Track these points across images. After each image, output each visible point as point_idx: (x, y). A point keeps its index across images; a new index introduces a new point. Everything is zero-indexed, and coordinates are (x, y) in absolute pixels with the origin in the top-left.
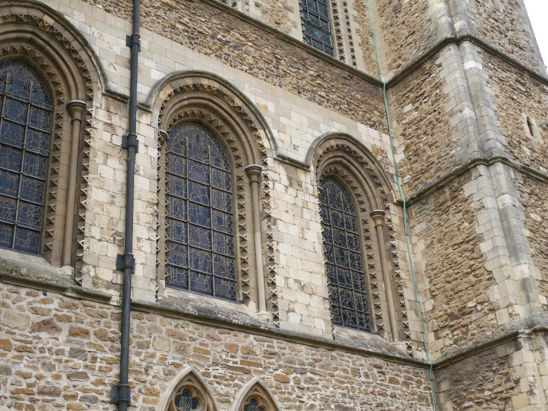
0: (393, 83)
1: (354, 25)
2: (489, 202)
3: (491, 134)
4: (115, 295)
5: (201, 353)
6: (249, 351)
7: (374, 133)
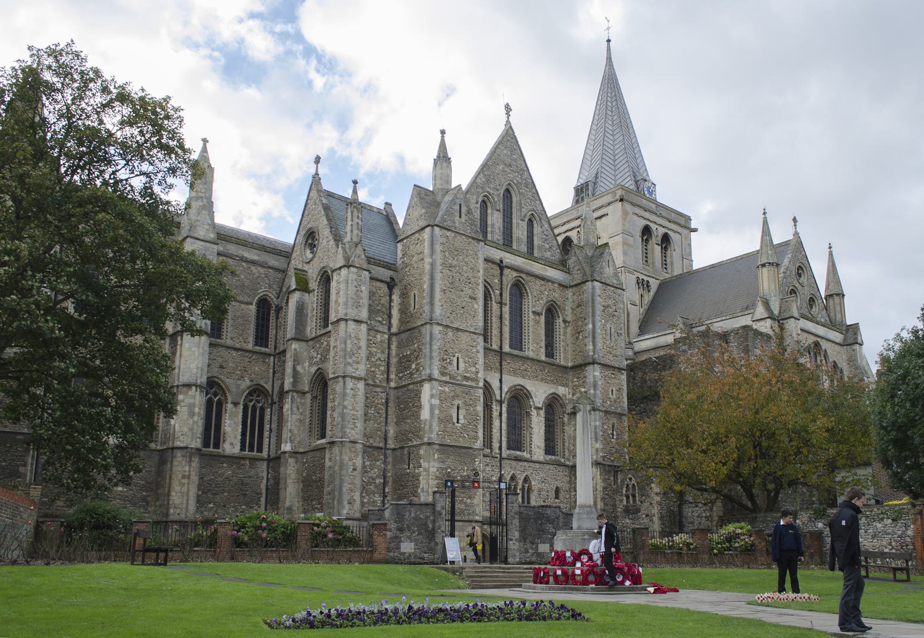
0: (573, 368)
1: (562, 343)
4: (498, 456)
6: (525, 466)
7: (563, 388)
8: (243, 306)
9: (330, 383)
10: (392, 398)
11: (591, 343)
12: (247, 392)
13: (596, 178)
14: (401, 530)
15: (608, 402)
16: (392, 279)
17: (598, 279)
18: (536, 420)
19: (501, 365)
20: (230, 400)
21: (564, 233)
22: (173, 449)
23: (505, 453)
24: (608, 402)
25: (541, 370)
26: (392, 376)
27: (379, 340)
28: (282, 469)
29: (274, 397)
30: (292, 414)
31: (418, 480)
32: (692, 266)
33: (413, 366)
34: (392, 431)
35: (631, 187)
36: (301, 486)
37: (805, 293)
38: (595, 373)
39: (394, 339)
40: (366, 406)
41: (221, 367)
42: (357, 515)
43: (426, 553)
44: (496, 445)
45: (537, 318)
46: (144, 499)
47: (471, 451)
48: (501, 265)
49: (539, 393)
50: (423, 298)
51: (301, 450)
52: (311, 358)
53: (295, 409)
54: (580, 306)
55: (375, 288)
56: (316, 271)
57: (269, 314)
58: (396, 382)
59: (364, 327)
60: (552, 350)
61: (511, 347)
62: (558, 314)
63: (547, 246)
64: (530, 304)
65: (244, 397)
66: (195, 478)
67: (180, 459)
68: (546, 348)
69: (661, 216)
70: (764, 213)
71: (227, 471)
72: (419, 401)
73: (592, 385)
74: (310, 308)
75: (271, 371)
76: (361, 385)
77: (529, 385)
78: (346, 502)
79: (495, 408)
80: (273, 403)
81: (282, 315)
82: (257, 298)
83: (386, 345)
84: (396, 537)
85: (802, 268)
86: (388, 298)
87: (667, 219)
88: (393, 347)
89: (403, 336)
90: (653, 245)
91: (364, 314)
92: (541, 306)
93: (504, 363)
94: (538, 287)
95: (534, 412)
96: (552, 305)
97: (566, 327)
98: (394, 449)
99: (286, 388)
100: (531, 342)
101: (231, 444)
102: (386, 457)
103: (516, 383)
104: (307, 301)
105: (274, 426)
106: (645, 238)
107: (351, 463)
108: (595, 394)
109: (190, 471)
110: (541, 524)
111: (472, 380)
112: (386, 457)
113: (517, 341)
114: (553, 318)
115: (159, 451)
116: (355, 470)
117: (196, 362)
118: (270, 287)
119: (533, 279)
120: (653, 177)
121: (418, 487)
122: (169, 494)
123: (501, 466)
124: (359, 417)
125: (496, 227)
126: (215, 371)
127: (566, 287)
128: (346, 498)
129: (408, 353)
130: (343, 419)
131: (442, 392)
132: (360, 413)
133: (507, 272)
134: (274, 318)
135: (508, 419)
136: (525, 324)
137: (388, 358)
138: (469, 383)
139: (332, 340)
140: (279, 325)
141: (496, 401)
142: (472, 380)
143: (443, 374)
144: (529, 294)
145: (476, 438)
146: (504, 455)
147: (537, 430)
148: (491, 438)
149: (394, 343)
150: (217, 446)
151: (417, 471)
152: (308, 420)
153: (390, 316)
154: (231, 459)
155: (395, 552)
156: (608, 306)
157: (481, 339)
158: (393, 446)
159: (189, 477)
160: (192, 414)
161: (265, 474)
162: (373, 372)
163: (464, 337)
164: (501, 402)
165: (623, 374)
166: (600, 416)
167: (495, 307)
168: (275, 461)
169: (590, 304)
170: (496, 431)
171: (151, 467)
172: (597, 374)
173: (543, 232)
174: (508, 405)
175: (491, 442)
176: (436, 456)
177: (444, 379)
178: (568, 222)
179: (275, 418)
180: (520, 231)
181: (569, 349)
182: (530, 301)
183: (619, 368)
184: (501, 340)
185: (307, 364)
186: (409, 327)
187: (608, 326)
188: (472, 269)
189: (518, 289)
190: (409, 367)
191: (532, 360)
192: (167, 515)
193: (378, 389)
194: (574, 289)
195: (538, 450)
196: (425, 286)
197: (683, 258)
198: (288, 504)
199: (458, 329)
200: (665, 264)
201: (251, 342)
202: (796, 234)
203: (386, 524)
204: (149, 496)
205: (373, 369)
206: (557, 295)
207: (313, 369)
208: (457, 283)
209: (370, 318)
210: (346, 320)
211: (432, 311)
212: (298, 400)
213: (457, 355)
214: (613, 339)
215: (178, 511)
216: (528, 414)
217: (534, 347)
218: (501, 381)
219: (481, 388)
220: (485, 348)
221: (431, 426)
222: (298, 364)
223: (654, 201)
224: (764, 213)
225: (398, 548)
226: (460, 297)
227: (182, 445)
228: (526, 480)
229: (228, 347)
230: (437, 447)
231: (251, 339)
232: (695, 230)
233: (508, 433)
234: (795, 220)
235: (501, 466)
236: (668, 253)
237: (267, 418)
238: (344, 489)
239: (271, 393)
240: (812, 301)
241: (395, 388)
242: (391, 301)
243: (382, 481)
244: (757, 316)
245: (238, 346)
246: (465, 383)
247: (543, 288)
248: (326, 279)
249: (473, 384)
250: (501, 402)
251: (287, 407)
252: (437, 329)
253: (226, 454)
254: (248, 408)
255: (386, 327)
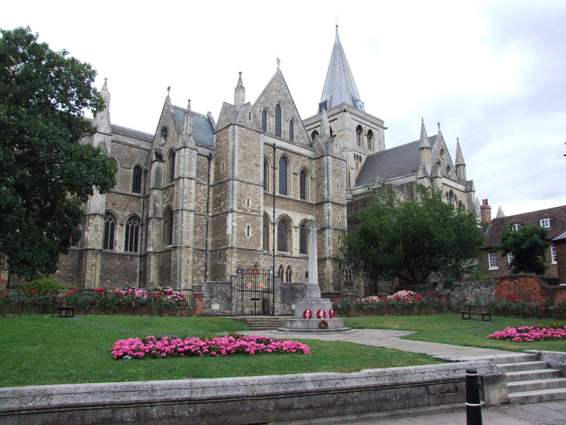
0: (316, 204)
1: (310, 191)
2: (327, 236)
3: (330, 223)
4: (273, 254)
5: (282, 261)
8: (126, 170)
9: (174, 213)
10: (210, 222)
11: (326, 191)
12: (128, 218)
13: (331, 99)
14: (212, 297)
15: (336, 224)
16: (210, 154)
17: (330, 154)
18: (295, 234)
19: (274, 203)
20: (118, 223)
21: (313, 128)
22: (86, 250)
23: (277, 252)
24: (336, 224)
25: (298, 206)
26: (210, 209)
27: (202, 189)
28: (148, 261)
29: (144, 221)
30: (153, 231)
31: (225, 268)
32: (385, 148)
33: (222, 204)
34: (210, 240)
35: (350, 104)
36: (159, 271)
37: (444, 164)
38: (328, 207)
39: (211, 188)
40: (195, 226)
41: (114, 204)
42: (190, 288)
43: (226, 310)
44: (271, 248)
45: (295, 176)
46: (71, 277)
47: (256, 252)
48: (274, 147)
49: (297, 218)
50: (228, 165)
51: (158, 251)
52: (164, 199)
53: (155, 228)
54: (320, 170)
55: (200, 159)
56: (167, 150)
57: (141, 175)
58: (212, 213)
59: (193, 182)
60: (304, 194)
61: (280, 193)
62: (308, 174)
63: (301, 136)
64: (291, 168)
65: (126, 221)
66: (99, 266)
67: (90, 255)
68: (301, 192)
69: (367, 120)
70: (422, 120)
71: (117, 262)
72: (226, 223)
73: (327, 214)
74: (163, 171)
75: (142, 206)
76: (192, 215)
77: (291, 214)
78: (183, 281)
79: (271, 227)
80: (143, 225)
81: (148, 175)
82: (134, 165)
83: (206, 192)
84: (208, 301)
85: (443, 151)
86: (208, 165)
87: (371, 122)
88: (211, 193)
89: (216, 187)
90: (363, 136)
91: (194, 174)
92: (297, 170)
93: (276, 202)
94: (296, 159)
95: (293, 230)
96: (304, 169)
97: (312, 182)
98: (211, 251)
99: (150, 216)
100: (292, 190)
101: (120, 247)
102: (206, 255)
103: (283, 213)
104: (162, 167)
105: (144, 237)
106: (358, 132)
107: (186, 259)
108: (329, 219)
109: (96, 262)
110: (293, 293)
111: (257, 212)
112: (206, 255)
113: (284, 189)
114: (305, 176)
115: (79, 251)
116: (188, 262)
117: (99, 202)
118: (142, 159)
119: (293, 154)
120: (362, 99)
121: (225, 272)
122: (85, 275)
123: (274, 260)
124: (191, 232)
125: (272, 125)
126: (110, 207)
127: (313, 159)
128: (183, 278)
129: (220, 196)
130: (182, 234)
131: (239, 219)
132: (191, 230)
133: (277, 150)
134: (144, 177)
135: (278, 234)
136: (288, 180)
137: (208, 199)
138: (255, 213)
139: (175, 189)
140: (146, 180)
141: (271, 223)
142: (257, 212)
143: (239, 208)
144: (291, 163)
145: (259, 245)
146: (276, 254)
147: (295, 240)
148: (268, 244)
149: (212, 191)
150: (111, 248)
151: (224, 263)
152: (162, 234)
153: (209, 175)
154: (120, 255)
155: (208, 309)
156: (336, 170)
157: (262, 189)
158: (211, 249)
159: (95, 265)
160: (96, 230)
161: (139, 264)
162: (199, 207)
163: (252, 188)
164: (274, 224)
165: (344, 208)
166: (332, 232)
167: (271, 170)
168: (144, 257)
169: (326, 169)
170: (271, 240)
171: (75, 259)
172: (330, 208)
173: (299, 128)
174: (279, 226)
175: (268, 246)
176: (235, 255)
177: (240, 211)
178: (315, 122)
179: (144, 233)
180: (285, 127)
181: (314, 194)
182: (291, 167)
183: (342, 205)
184: (274, 189)
185: (161, 203)
186: (220, 182)
187: (336, 181)
188: (257, 149)
189: (285, 160)
190: (220, 204)
191: (293, 200)
192: (84, 286)
193: (202, 217)
194: (317, 160)
195: (296, 251)
196: (229, 159)
197: (380, 143)
198: (151, 281)
199: (248, 183)
200: (370, 147)
201: (130, 190)
202: (439, 132)
203: (202, 294)
204: (74, 276)
205: (199, 206)
206: (307, 163)
207: (165, 206)
208: (248, 157)
209: (197, 177)
210: (183, 178)
211: (233, 172)
212: (157, 223)
213: (247, 197)
214: (339, 188)
215: (90, 284)
216: (290, 231)
217: (294, 192)
218: (274, 212)
219: (262, 216)
220: (264, 194)
221: (232, 238)
222: (157, 202)
223: (364, 112)
224: (422, 120)
225: (210, 307)
226: (249, 165)
227: (92, 248)
228: (289, 268)
229: (117, 193)
230: (236, 250)
231: (131, 188)
232: (386, 128)
233: (279, 241)
234: (439, 124)
235: (274, 260)
236: (372, 140)
237: (140, 232)
238: (182, 273)
239: (141, 218)
240: (448, 168)
241: (212, 216)
242: (209, 167)
243: (204, 269)
244: (419, 176)
245: (123, 192)
246: (252, 213)
247: (299, 160)
248: (172, 154)
249: (257, 214)
250: (274, 224)
251: (150, 226)
252: (236, 183)
253: (116, 253)
254: (129, 227)
255: (207, 182)
